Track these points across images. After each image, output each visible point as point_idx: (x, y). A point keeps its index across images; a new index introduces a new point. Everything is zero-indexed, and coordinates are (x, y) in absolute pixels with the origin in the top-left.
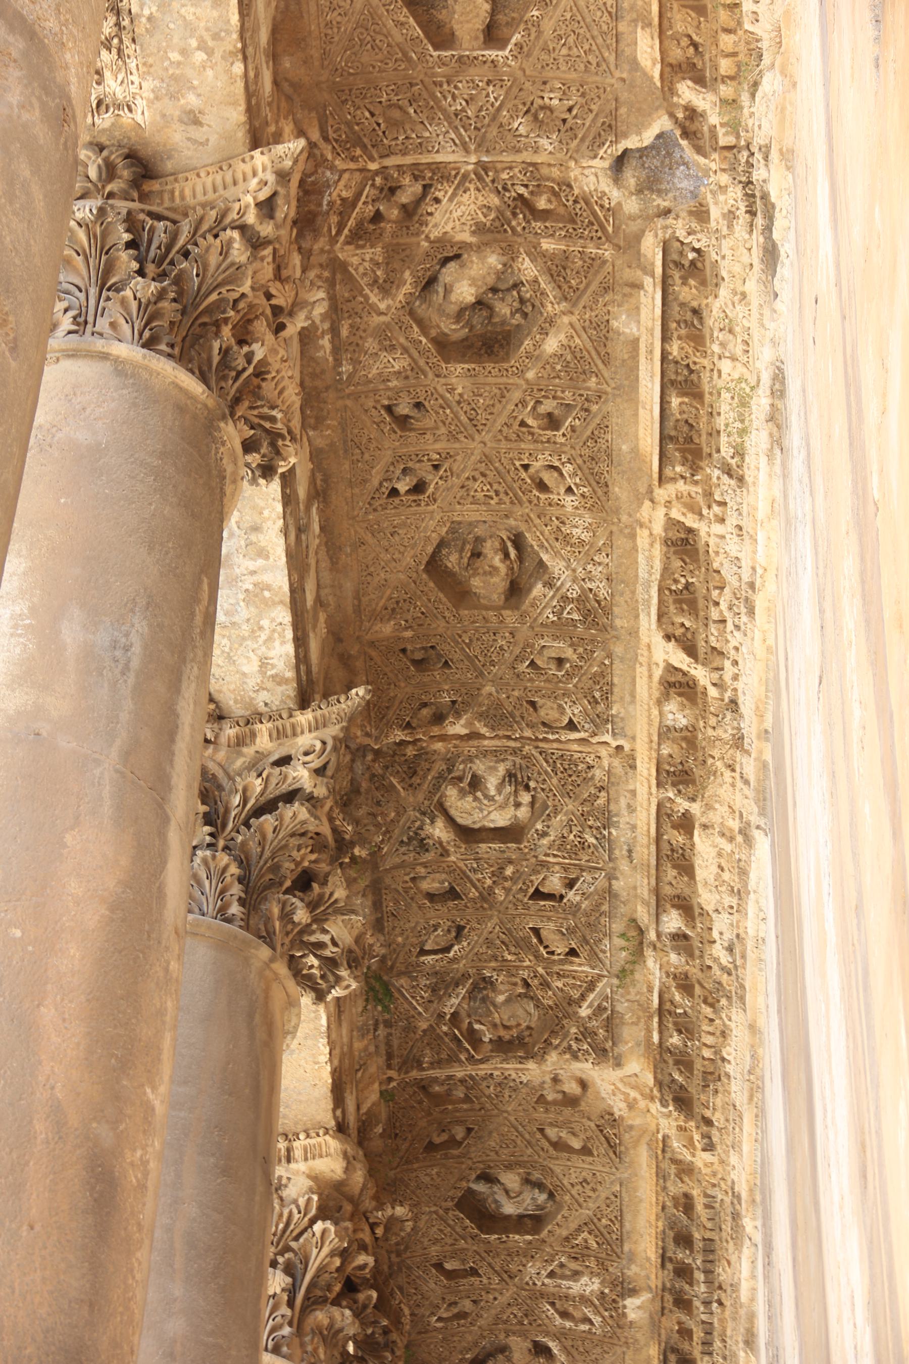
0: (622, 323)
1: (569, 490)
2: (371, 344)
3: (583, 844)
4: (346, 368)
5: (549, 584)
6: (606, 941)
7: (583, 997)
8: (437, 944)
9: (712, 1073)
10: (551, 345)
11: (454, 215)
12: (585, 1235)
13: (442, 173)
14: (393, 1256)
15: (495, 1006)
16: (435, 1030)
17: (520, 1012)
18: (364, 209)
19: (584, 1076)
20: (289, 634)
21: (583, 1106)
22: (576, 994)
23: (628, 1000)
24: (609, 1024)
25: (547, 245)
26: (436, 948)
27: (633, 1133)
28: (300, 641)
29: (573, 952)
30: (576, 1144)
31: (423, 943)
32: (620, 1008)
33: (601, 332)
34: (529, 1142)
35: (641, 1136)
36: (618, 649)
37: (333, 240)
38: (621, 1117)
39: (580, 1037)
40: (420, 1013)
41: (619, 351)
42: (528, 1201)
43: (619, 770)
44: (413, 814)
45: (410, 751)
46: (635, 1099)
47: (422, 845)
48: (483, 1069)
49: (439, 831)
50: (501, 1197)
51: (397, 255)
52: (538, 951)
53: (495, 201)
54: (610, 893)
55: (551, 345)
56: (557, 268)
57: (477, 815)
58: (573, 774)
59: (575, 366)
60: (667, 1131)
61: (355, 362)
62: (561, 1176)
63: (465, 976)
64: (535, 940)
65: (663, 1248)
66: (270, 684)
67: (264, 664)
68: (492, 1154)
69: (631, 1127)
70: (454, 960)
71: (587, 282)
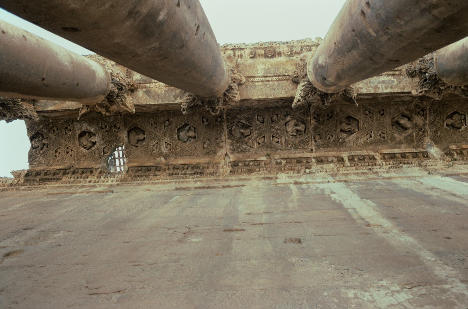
0: (403, 146)
1: (367, 139)
2: (396, 107)
3: (288, 145)
4: (393, 103)
5: (347, 137)
7: (248, 146)
10: (396, 135)
11: (419, 120)
12: (180, 149)
13: (426, 118)
18: (421, 106)
20: (368, 93)
21: (217, 147)
22: (248, 144)
24: (242, 151)
25: (414, 134)
28: (367, 94)
29: (259, 144)
30: (205, 146)
31: (260, 116)
33: (401, 143)
36: (335, 149)
37: (417, 101)
41: (398, 146)
43: (308, 150)
44: (293, 114)
45: (309, 113)
47: (286, 116)
48: (225, 128)
49: (289, 118)
50: (184, 132)
51: (412, 111)
53: (421, 126)
54: (277, 150)
55: (396, 135)
56: (411, 136)
57: (290, 125)
58: (305, 142)
59: (393, 139)
61: (394, 104)
63: (251, 124)
66: (356, 89)
67: (361, 88)
69: (215, 156)
70: (255, 122)
71: (409, 141)
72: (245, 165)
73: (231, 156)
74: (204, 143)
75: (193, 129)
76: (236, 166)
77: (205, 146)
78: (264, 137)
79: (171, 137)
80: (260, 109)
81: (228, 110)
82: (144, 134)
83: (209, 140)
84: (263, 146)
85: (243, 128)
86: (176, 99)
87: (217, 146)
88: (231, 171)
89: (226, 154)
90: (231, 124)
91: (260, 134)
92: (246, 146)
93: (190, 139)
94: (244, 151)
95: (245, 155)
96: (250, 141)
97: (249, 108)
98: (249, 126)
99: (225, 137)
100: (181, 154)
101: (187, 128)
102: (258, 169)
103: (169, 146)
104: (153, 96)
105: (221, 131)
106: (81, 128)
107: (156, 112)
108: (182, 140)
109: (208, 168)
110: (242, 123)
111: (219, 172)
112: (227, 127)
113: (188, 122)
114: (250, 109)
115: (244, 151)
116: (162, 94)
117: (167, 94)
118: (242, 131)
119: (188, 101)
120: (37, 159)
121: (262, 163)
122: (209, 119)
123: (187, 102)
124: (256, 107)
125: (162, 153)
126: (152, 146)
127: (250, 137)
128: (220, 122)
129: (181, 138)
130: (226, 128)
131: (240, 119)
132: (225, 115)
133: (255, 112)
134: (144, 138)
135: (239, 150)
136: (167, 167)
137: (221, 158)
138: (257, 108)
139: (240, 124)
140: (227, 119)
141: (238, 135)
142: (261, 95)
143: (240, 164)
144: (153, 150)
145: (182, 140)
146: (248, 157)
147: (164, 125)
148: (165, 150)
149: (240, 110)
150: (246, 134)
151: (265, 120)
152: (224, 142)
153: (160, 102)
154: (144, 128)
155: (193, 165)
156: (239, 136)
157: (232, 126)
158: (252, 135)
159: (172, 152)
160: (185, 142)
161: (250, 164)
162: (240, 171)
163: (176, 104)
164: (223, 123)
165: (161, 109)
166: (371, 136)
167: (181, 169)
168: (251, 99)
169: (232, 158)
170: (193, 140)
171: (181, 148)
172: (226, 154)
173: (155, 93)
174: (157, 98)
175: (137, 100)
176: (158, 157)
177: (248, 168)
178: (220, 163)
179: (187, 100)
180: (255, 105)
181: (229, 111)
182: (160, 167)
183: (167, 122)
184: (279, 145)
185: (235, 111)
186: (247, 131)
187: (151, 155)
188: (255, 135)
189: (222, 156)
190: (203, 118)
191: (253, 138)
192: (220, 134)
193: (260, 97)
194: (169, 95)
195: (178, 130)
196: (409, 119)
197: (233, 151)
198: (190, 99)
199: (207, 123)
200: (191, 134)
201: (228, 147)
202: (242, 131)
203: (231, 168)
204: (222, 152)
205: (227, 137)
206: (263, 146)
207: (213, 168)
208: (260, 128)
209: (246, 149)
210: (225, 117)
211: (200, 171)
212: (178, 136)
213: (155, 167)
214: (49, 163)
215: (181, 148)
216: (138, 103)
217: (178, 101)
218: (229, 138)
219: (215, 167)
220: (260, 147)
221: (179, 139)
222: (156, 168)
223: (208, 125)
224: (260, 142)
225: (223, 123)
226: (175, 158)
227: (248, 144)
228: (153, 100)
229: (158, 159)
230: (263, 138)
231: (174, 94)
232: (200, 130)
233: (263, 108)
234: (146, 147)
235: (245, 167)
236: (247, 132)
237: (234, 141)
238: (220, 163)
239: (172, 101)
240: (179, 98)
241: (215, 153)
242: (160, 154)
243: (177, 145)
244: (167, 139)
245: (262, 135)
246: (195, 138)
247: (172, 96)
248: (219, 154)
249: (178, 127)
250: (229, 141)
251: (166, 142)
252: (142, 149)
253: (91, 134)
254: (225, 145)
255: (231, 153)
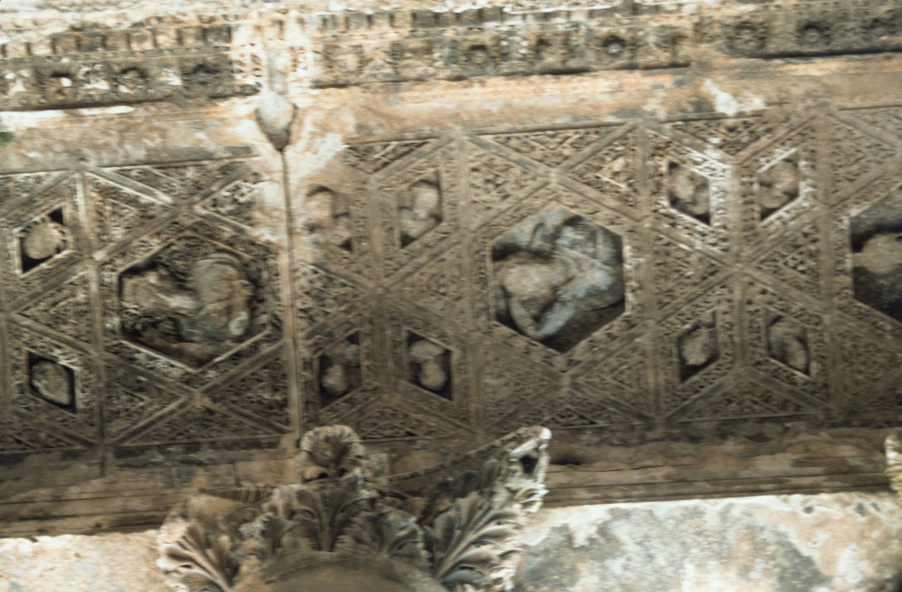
6: (19, 177)
7: (133, 201)
8: (58, 387)
9: (78, 40)
14: (651, 435)
15: (199, 309)
16: (215, 387)
17: (209, 277)
19: (305, 191)
21: (347, 189)
22: (131, 212)
23: (120, 144)
26: (65, 386)
27: (372, 123)
29: (57, 216)
32: (141, 154)
34: (434, 256)
35: (377, 114)
38: (347, 141)
39: (208, 201)
40: (182, 406)
42: (576, 253)
46: (315, 124)
50: (580, 288)
52: (63, 262)
60: (307, 83)
62: (492, 213)
64: (44, 266)
65: (543, 73)
68: (459, 305)
69: (360, 127)
72: (143, 74)
73: (247, 132)
74: (437, 218)
75: (518, 312)
76: (203, 67)
77: (427, 197)
78: (28, 263)
79: (665, 257)
80: (56, 454)
81: (273, 445)
82: (859, 272)
83: (406, 240)
84: (29, 204)
85: (174, 317)
86: (603, 530)
87: (347, 199)
88: (227, 33)
89: (281, 141)
90: (255, 347)
91: (56, 279)
92: (145, 199)
93: (538, 243)
94: (163, 166)
95: (155, 142)
96: (118, 233)
97: (129, 456)
98: (133, 334)
99: (296, 260)
100: (594, 136)
101: (556, 321)
102: (42, 50)
103: (685, 191)
104: (759, 548)
105: (319, 298)
107: (770, 429)
108: (592, 237)
109: (396, 52)
110: (178, 355)
111: (313, 29)
112: (277, 325)
113: (547, 359)
114: (122, 453)
115: (163, 166)
116: (701, 566)
117: (661, 561)
118: (179, 302)
119: (492, 528)
121: (18, 88)
122: (404, 384)
123: (498, 518)
124: (82, 467)
125: (729, 147)
126: (805, 189)
127: (123, 265)
128: (325, 363)
129: (604, 249)
130: (290, 321)
131: (188, 380)
132: (294, 411)
133: (89, 433)
134: (858, 242)
135: (191, 173)
136: (686, 50)
137: (319, 116)
138: (75, 455)
139: (192, 348)
140: (278, 382)
141: (209, 271)
142: (21, 558)
143: (176, 81)
144: (791, 161)
145: (592, 237)
146: (127, 127)
147: (713, 335)
148: (712, 164)
149: (194, 447)
150: (152, 278)
151: (21, 376)
152: (300, 222)
153: (712, 507)
154: (861, 316)
155: (505, 67)
156: (204, 263)
157: (249, 332)
158: (111, 278)
159: (659, 150)
160: (573, 222)
161: (102, 85)
162: (166, 40)
163: (602, 494)
164: (305, 353)
165: (730, 446)
167: (578, 40)
168: (96, 530)
169: (236, 123)
170: (523, 233)
171: (597, 185)
172: (281, 141)
173: (745, 571)
174: (731, 536)
175: (873, 522)
176: (757, 114)
177: (120, 56)
178: (319, 85)
179: (499, 536)
180: (87, 478)
181: (262, 436)
182: (732, 50)
183: (695, 355)
185: (228, 437)
186: (148, 304)
187: (805, 131)
188: (90, 272)
189: (308, 127)
190: (445, 390)
191: (99, 256)
192: (330, 280)
193: (24, 545)
194: (651, 557)
195: (619, 304)
197: (233, 167)
198: (479, 542)
199: (420, 351)
200: (527, 280)
201: (269, 193)
202: (179, 302)
203: (234, 55)
204: (315, 156)
205: (283, 261)
206: (29, 204)
207: (358, 50)
208: (57, 321)
209: (147, 179)
210: (295, 394)
211: (449, 33)
212: (618, 259)
213: (771, 48)
215: (597, 185)
216: (868, 501)
217: (582, 520)
218: (268, 251)
219: (351, 61)
220: (52, 192)
221: (616, 242)
222: (763, 40)
223: (413, 339)
224: (53, 232)
225: (305, 353)
226: (634, 112)
227: (131, 212)
228: (760, 520)
229: (757, 103)
230: (34, 254)
231: (616, 565)
232: (464, 304)
233: (34, 460)
234: (846, 188)
235: (138, 59)
236: (145, 295)
237: (228, 233)
238: (319, 85)
239: (626, 515)
240: (580, 540)
241: (358, 151)
242: (740, 136)
243: (624, 199)
245: (44, 276)
246: (504, 253)
247: (630, 547)
248: (333, 144)
249: (616, 326)
250: (263, 234)
251: (705, 218)
252: (874, 171)
254: (297, 203)
255: (247, 150)
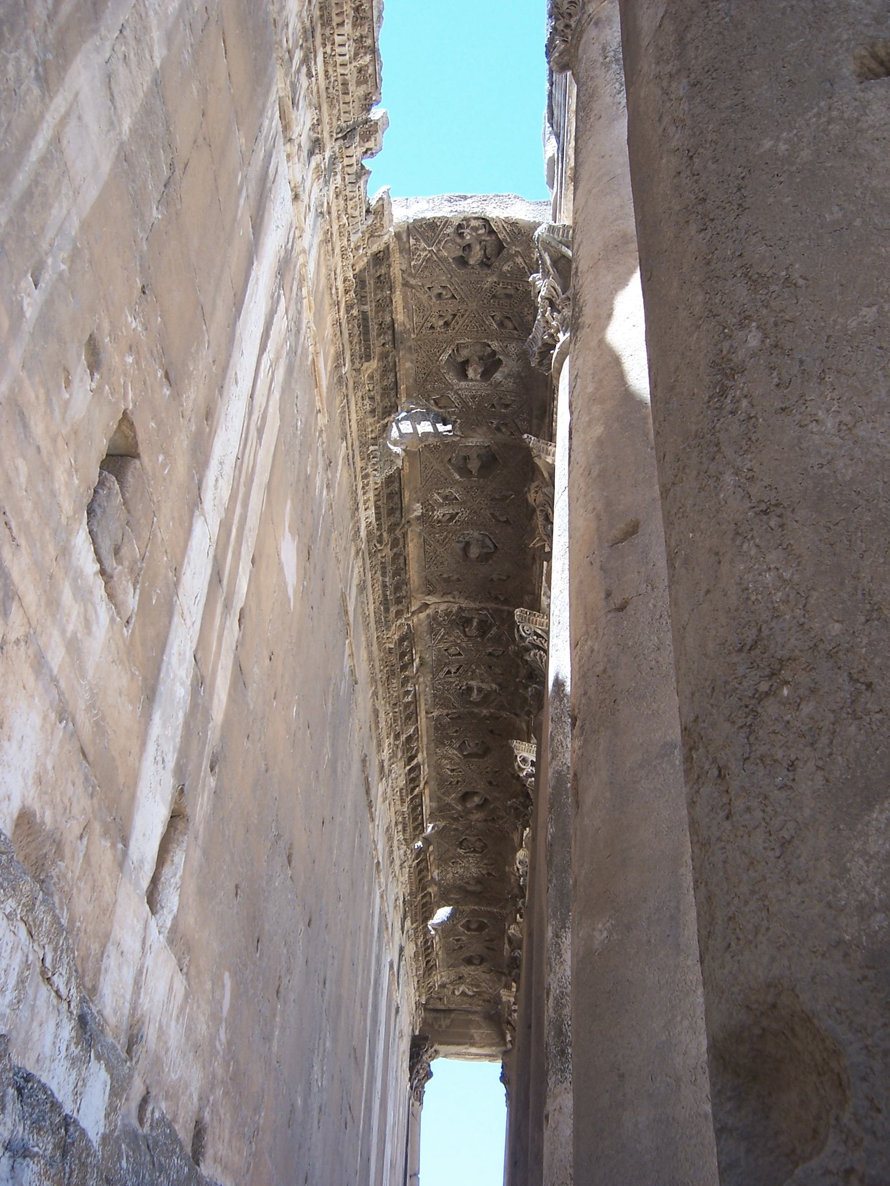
69: (422, 593)
106: (507, 355)
120: (423, 245)
159: (433, 527)
166: (452, 771)
184: (442, 675)
196: (480, 807)
201: (443, 607)
214: (410, 274)
236: (472, 630)
244: (464, 515)
253: (487, 374)
